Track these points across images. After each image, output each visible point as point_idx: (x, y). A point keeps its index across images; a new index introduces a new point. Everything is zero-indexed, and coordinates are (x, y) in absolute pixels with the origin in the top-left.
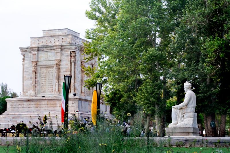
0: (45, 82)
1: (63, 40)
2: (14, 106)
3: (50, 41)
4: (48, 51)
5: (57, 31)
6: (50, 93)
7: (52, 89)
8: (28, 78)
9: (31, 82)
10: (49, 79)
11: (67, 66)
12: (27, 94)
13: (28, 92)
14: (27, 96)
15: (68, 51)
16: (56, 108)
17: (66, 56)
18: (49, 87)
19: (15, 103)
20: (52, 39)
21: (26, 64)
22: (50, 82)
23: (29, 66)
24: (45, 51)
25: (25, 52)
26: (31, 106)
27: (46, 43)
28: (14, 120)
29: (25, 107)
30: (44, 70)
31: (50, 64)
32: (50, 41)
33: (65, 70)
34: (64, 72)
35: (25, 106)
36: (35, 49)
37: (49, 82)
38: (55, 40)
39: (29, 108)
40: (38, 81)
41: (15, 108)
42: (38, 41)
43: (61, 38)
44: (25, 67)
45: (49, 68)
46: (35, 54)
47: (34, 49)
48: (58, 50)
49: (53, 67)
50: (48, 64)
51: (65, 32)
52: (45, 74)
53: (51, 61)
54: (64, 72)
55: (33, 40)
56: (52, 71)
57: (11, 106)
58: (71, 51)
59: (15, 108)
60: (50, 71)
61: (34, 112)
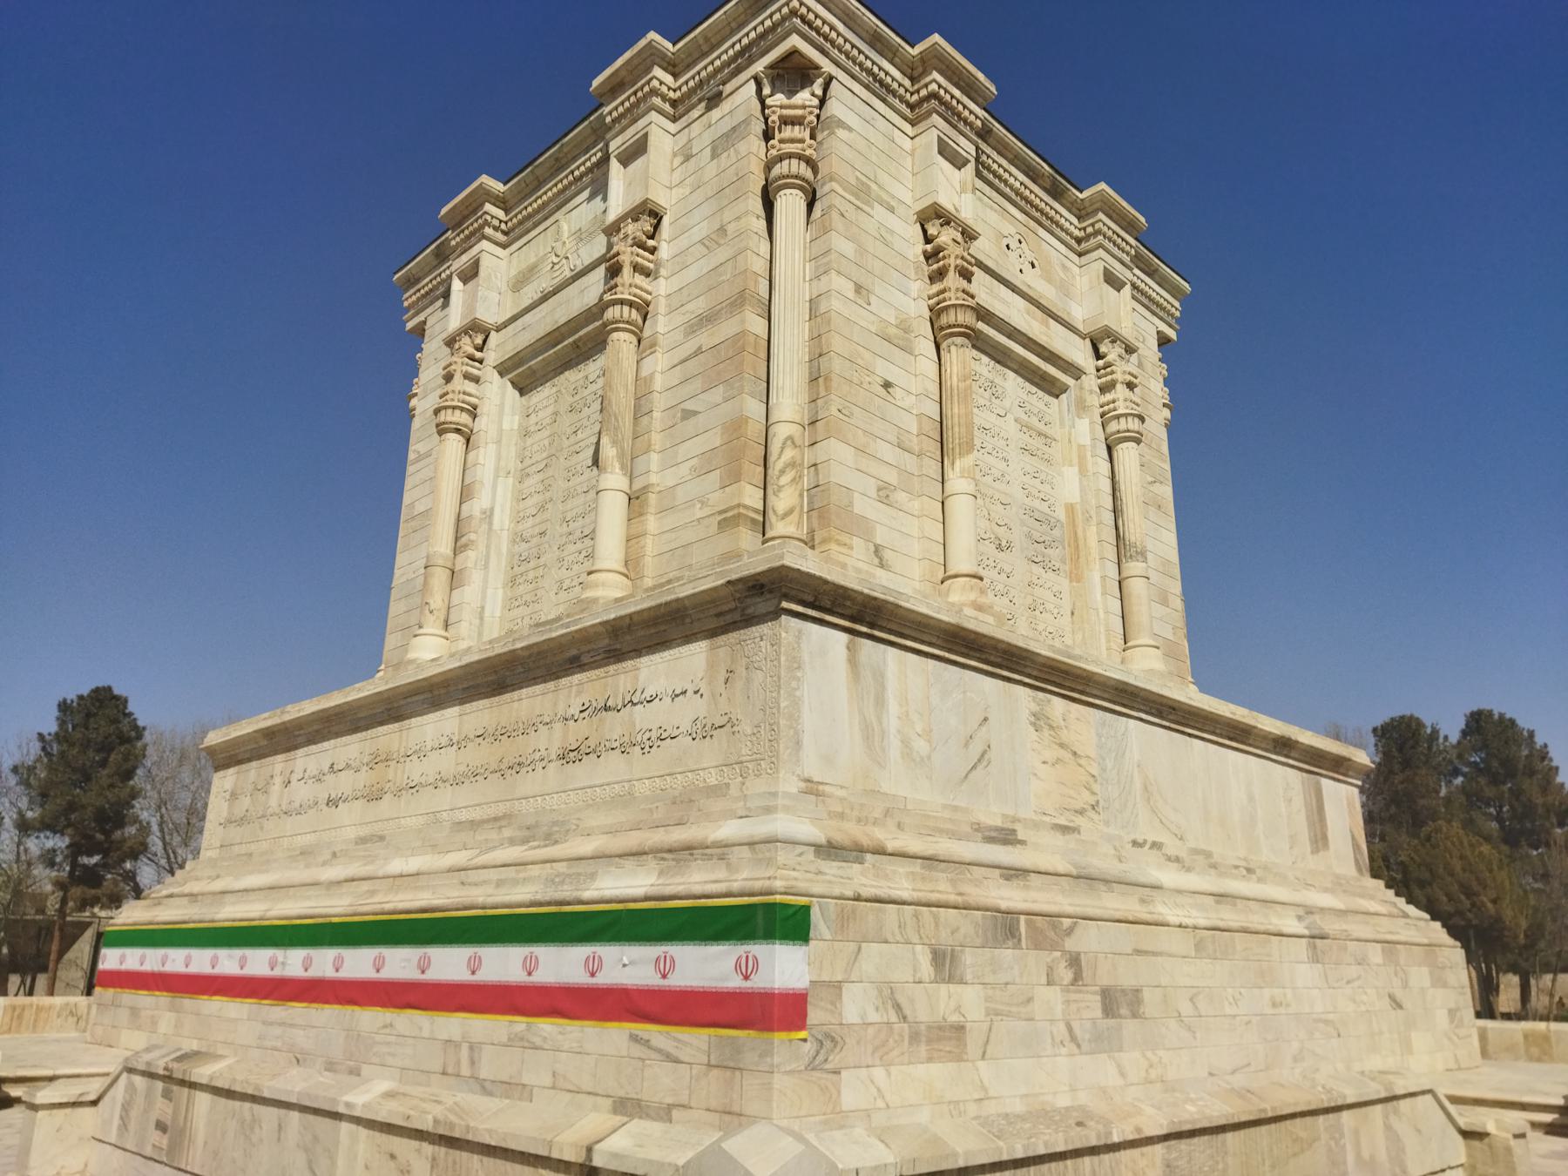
33: (700, 306)
40: (488, 515)
58: (759, 67)
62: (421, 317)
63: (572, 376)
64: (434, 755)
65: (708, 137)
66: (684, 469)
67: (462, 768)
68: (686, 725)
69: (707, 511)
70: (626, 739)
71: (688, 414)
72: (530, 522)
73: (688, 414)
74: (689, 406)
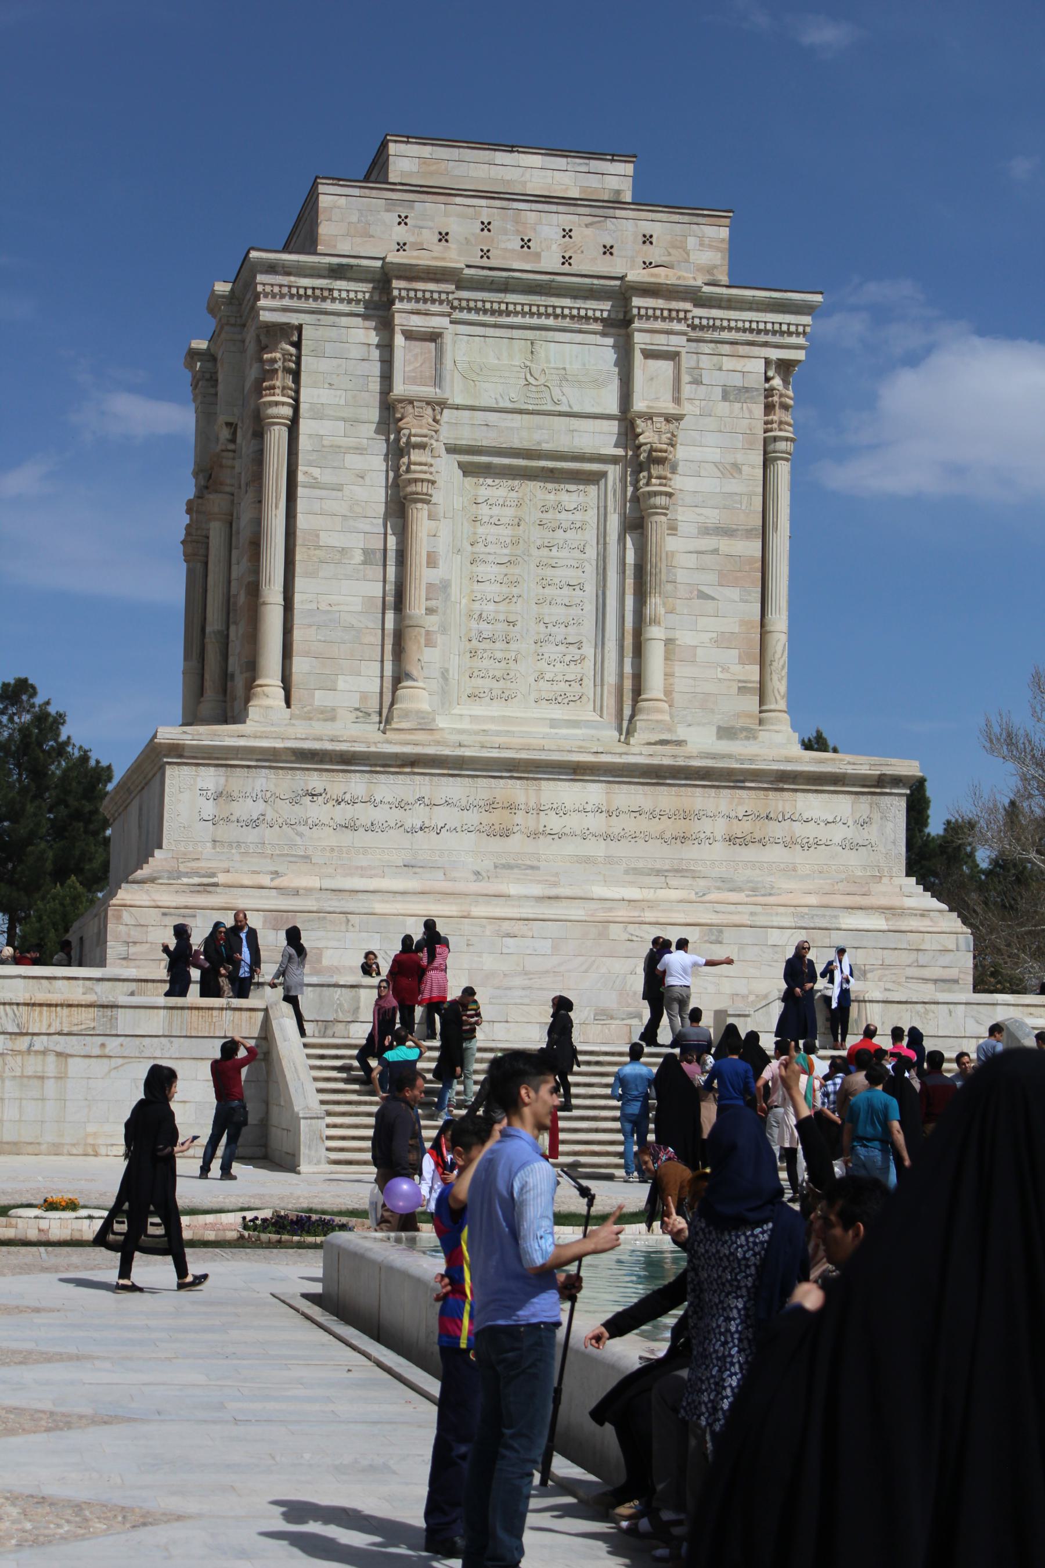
0: (502, 607)
1: (654, 254)
3: (526, 244)
4: (551, 322)
5: (536, 160)
6: (558, 712)
7: (573, 672)
8: (343, 551)
10: (545, 583)
11: (734, 486)
12: (321, 699)
13: (341, 684)
14: (333, 719)
15: (742, 350)
16: (691, 853)
17: (725, 397)
18: (551, 650)
19: (264, 780)
20: (547, 228)
21: (318, 415)
22: (558, 613)
23: (351, 442)
24: (518, 320)
25: (312, 304)
26: (441, 816)
27: (485, 254)
29: (371, 827)
30: (496, 490)
31: (563, 443)
32: (526, 244)
33: (712, 516)
34: (706, 531)
35: (366, 814)
36: (431, 286)
37: (546, 609)
38: (567, 233)
39: (413, 831)
40: (445, 586)
41: (254, 824)
42: (403, 221)
43: (628, 227)
44: (304, 443)
46: (434, 337)
48: (659, 325)
50: (545, 446)
51: (613, 183)
52: (506, 533)
53: (575, 422)
54: (706, 531)
55: (343, 200)
56: (578, 516)
57: (209, 809)
58: (775, 354)
59: (254, 824)
60: (559, 507)
61: (477, 873)
62: (294, 319)
63: (533, 488)
64: (576, 816)
65: (720, 378)
66: (706, 637)
67: (616, 830)
68: (837, 840)
69: (726, 676)
70: (788, 839)
71: (703, 596)
72: (491, 607)
73: (703, 596)
74: (705, 589)
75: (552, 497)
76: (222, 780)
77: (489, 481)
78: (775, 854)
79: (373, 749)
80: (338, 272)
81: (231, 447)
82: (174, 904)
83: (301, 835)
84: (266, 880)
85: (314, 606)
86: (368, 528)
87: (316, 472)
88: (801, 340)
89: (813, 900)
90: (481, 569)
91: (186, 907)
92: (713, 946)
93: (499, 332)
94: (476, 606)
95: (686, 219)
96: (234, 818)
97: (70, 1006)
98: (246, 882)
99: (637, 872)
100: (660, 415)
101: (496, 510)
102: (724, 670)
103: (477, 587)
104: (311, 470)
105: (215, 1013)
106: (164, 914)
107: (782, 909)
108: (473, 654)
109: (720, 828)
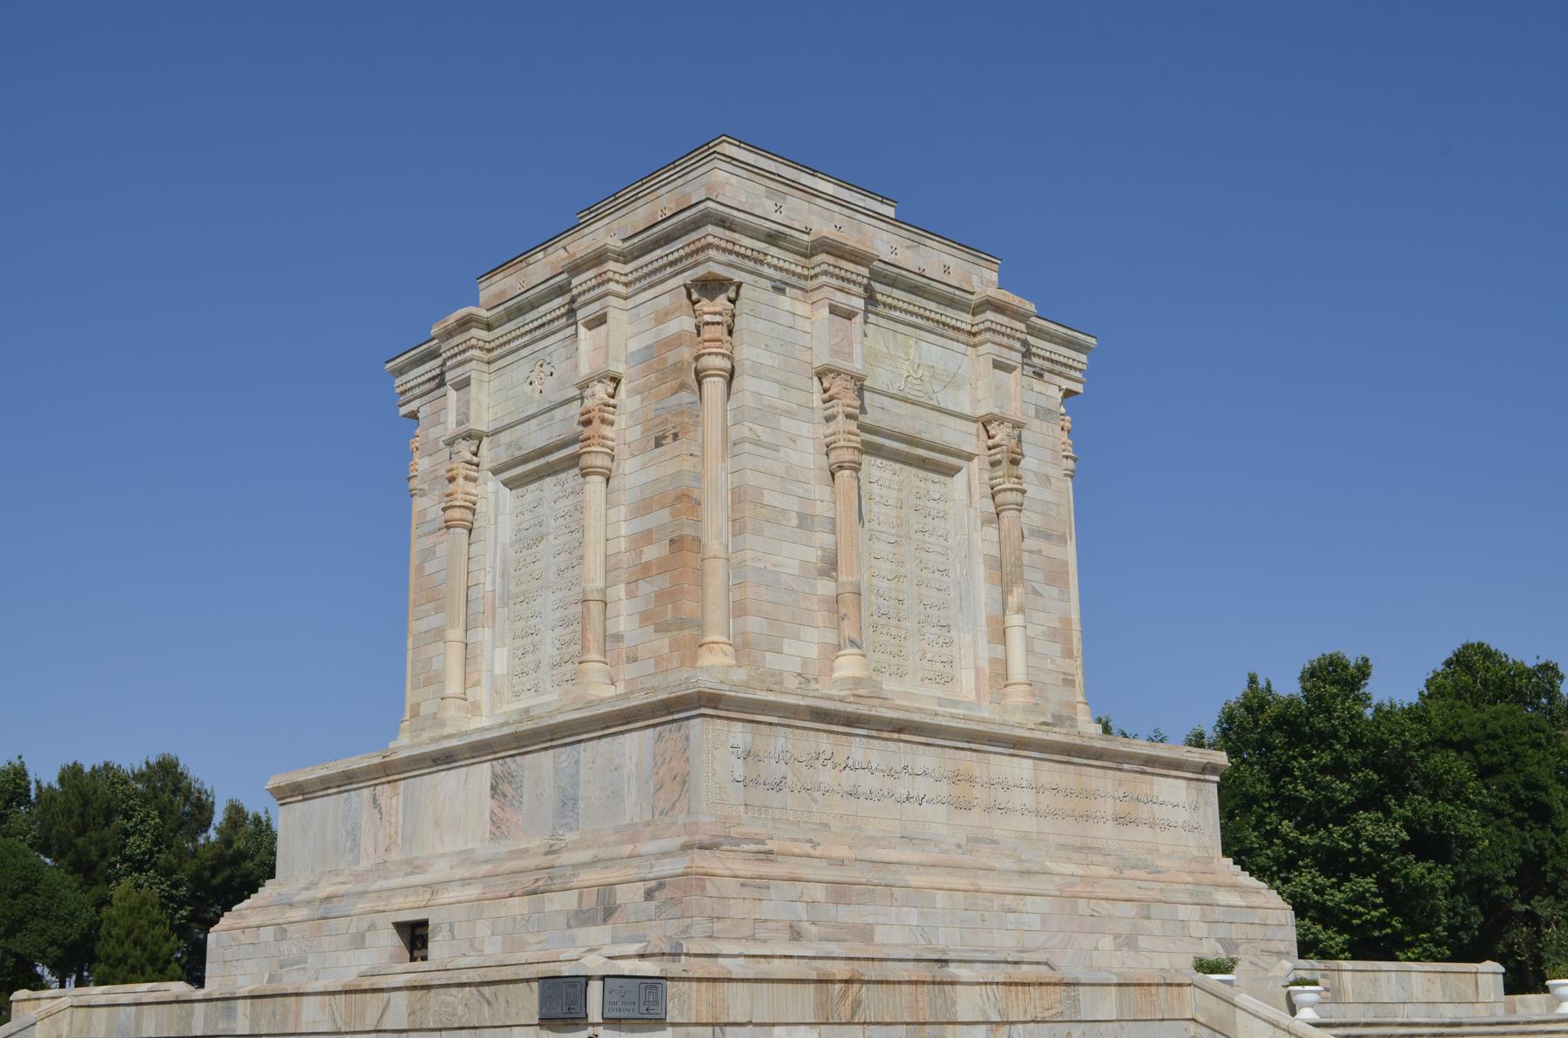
0: (893, 584)
2: (772, 770)
8: (784, 512)
9: (813, 555)
12: (771, 661)
13: (786, 649)
26: (922, 786)
28: (845, 914)
35: (868, 782)
36: (851, 267)
41: (778, 786)
45: (922, 473)
46: (849, 315)
47: (844, 264)
49: (950, 471)
50: (925, 436)
56: (941, 506)
57: (739, 770)
62: (737, 276)
72: (885, 584)
75: (922, 484)
76: (749, 737)
77: (879, 461)
78: (1143, 833)
79: (873, 712)
80: (773, 238)
81: (612, 401)
82: (749, 874)
83: (815, 800)
84: (807, 848)
85: (761, 565)
86: (801, 492)
87: (759, 429)
88: (1078, 375)
89: (1188, 878)
90: (877, 545)
91: (760, 877)
92: (1146, 922)
93: (891, 325)
94: (875, 581)
95: (971, 258)
96: (761, 780)
97: (1041, 984)
98: (797, 851)
99: (1063, 847)
100: (1010, 421)
101: (884, 492)
102: (1053, 662)
103: (875, 563)
104: (755, 427)
105: (1153, 989)
106: (743, 885)
107: (1177, 886)
108: (875, 627)
109: (1107, 807)
